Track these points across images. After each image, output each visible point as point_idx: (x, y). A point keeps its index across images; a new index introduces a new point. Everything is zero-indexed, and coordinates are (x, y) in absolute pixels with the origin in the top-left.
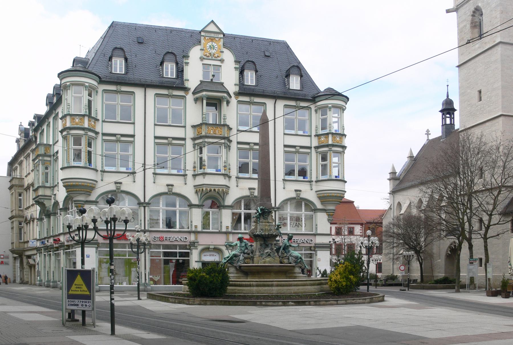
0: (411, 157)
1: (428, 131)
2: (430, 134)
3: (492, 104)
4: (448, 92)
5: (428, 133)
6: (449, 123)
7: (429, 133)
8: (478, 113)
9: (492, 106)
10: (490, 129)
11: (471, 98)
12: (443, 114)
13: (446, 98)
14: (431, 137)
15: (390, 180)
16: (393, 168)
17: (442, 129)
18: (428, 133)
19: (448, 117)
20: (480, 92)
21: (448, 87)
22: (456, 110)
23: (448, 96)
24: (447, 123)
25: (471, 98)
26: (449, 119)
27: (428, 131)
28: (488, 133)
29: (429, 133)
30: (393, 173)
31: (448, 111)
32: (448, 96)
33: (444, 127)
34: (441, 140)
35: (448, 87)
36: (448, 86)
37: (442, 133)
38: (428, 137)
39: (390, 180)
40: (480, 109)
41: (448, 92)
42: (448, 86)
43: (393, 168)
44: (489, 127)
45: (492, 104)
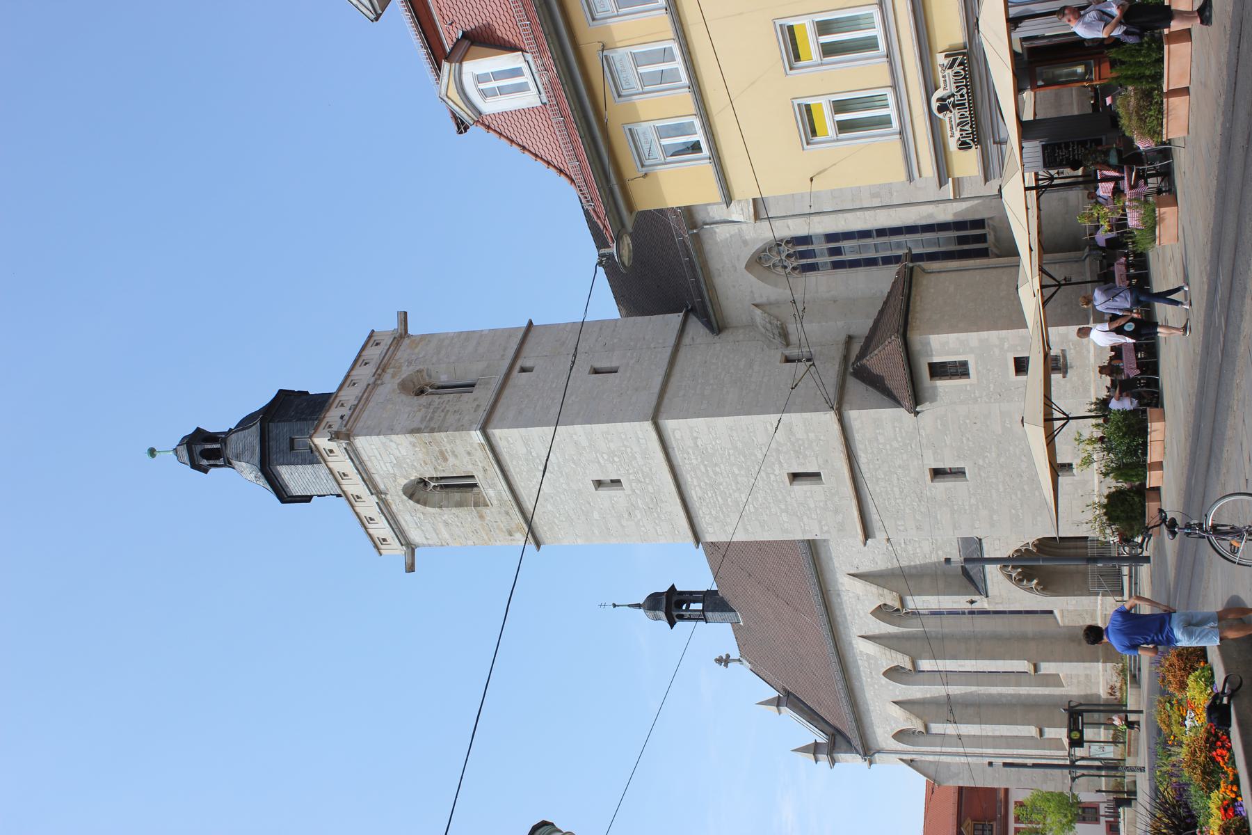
0: (778, 702)
1: (719, 661)
2: (728, 656)
3: (629, 450)
4: (629, 606)
5: (724, 661)
6: (702, 604)
7: (724, 658)
8: (651, 490)
9: (632, 449)
10: (691, 452)
11: (613, 507)
12: (681, 618)
13: (642, 611)
14: (735, 654)
15: (833, 762)
16: (804, 750)
17: (715, 621)
18: (724, 661)
19: (688, 606)
20: (599, 484)
21: (618, 606)
22: (673, 585)
23: (639, 606)
24: (701, 608)
25: (613, 507)
26: (692, 604)
27: (719, 661)
28: (699, 460)
29: (724, 658)
30: (815, 749)
31: (673, 606)
32: (639, 606)
33: (709, 615)
34: (741, 623)
35: (618, 606)
36: (615, 606)
37: (724, 621)
38: (734, 660)
39: (833, 762)
40: (641, 482)
41: (629, 606)
42: (615, 606)
43: (804, 750)
44: (685, 455)
45: (629, 450)
